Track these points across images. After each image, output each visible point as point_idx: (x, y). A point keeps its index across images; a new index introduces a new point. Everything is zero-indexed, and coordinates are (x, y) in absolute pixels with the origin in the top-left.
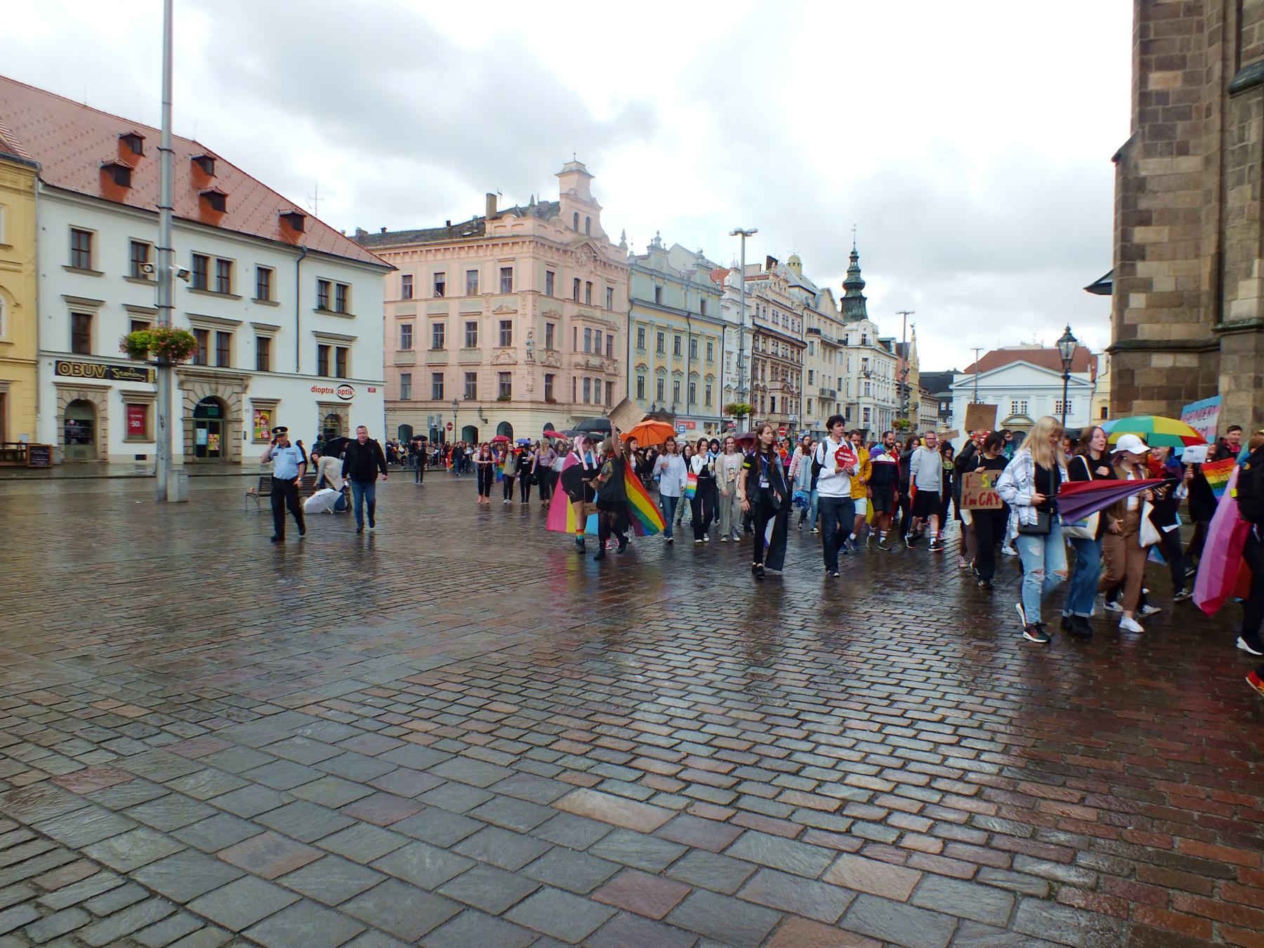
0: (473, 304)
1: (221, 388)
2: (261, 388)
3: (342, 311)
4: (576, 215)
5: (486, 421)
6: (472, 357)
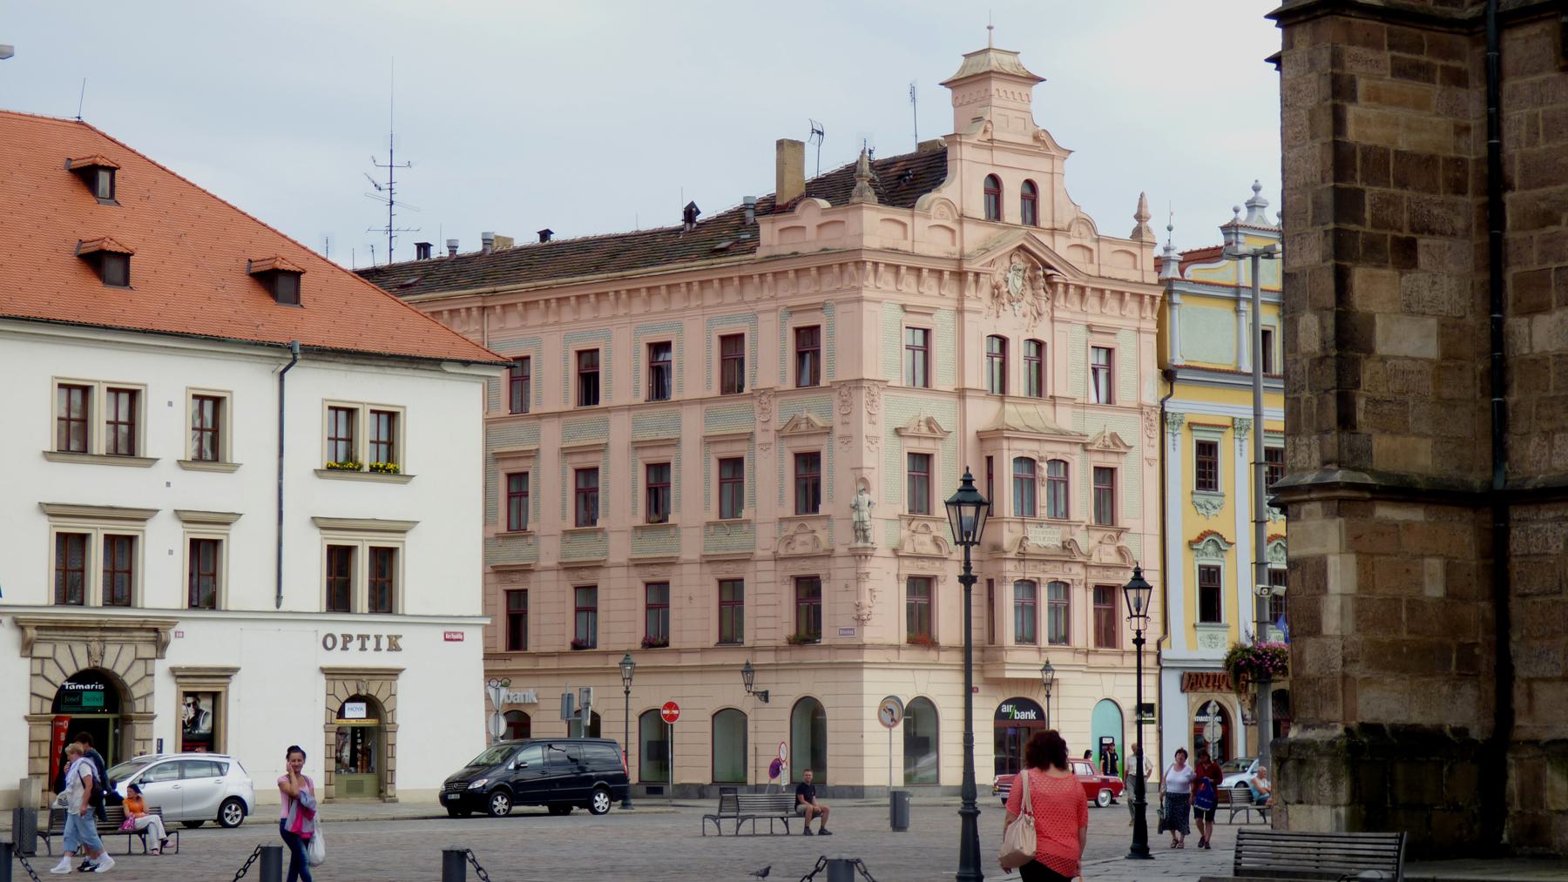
0: (734, 417)
1: (111, 650)
2: (198, 643)
3: (388, 466)
4: (994, 180)
5: (765, 696)
6: (733, 543)
